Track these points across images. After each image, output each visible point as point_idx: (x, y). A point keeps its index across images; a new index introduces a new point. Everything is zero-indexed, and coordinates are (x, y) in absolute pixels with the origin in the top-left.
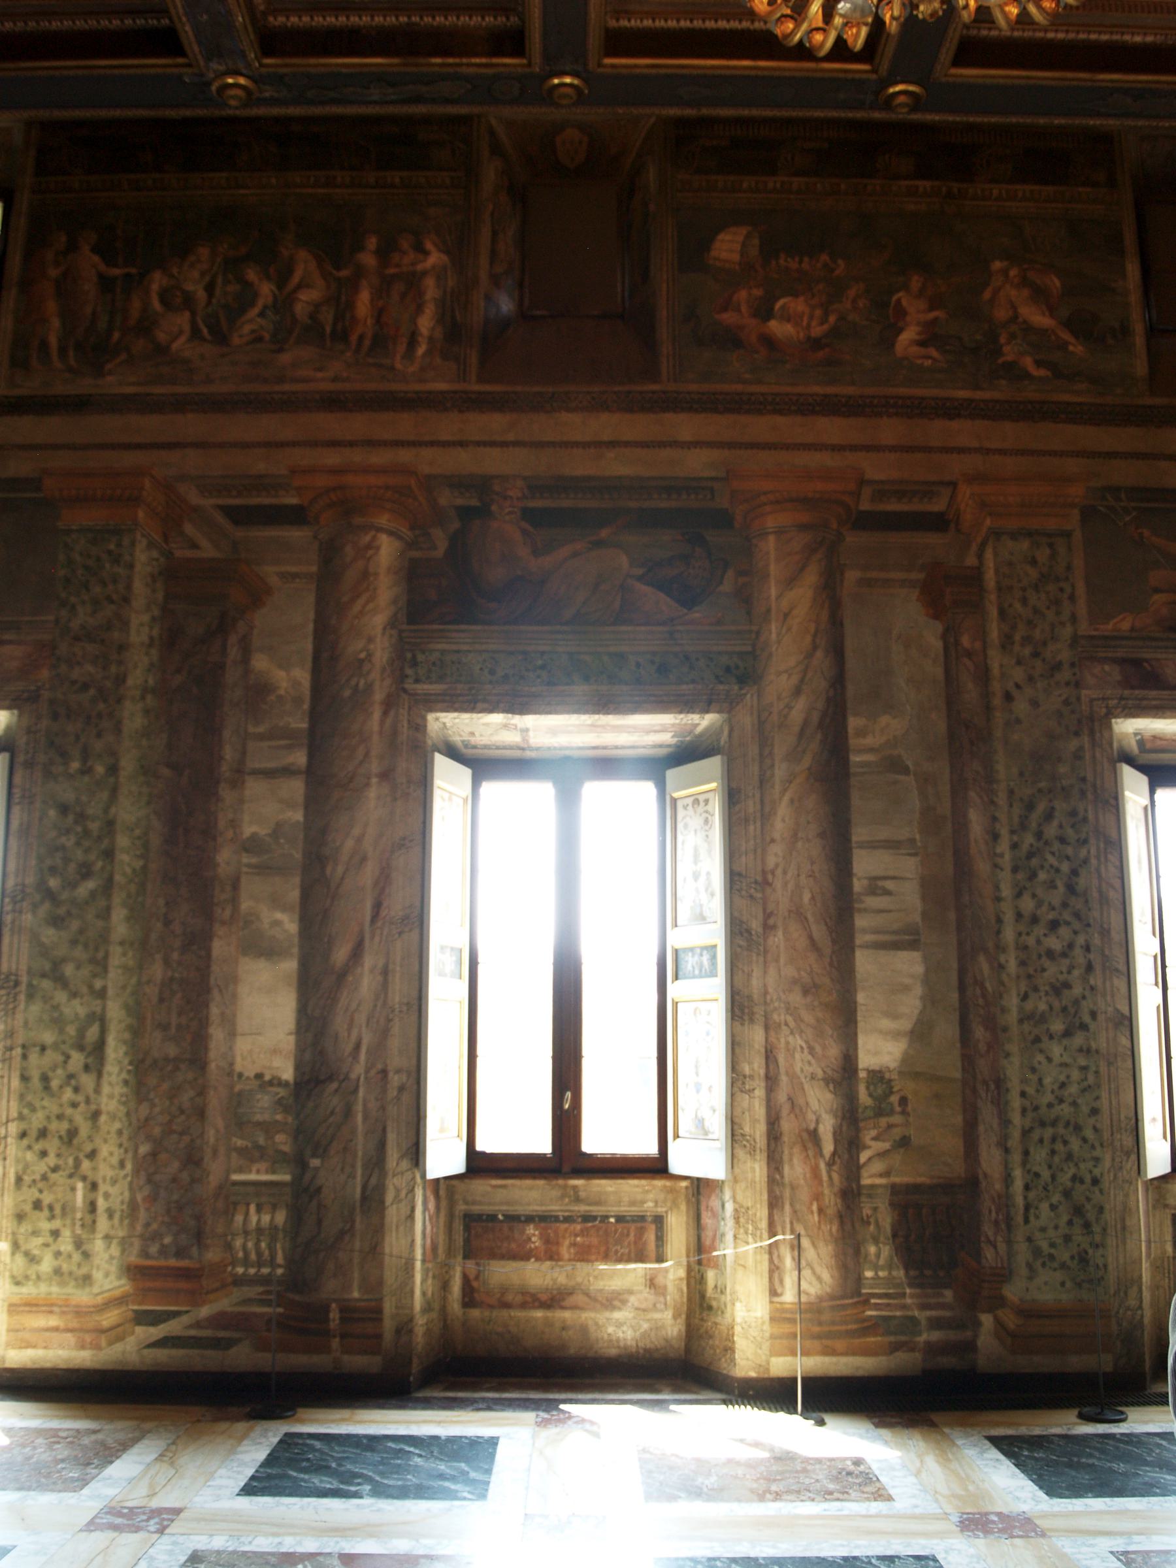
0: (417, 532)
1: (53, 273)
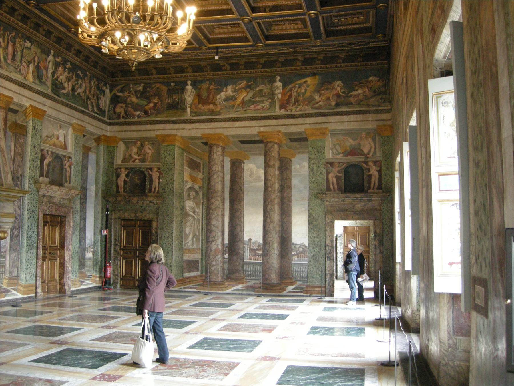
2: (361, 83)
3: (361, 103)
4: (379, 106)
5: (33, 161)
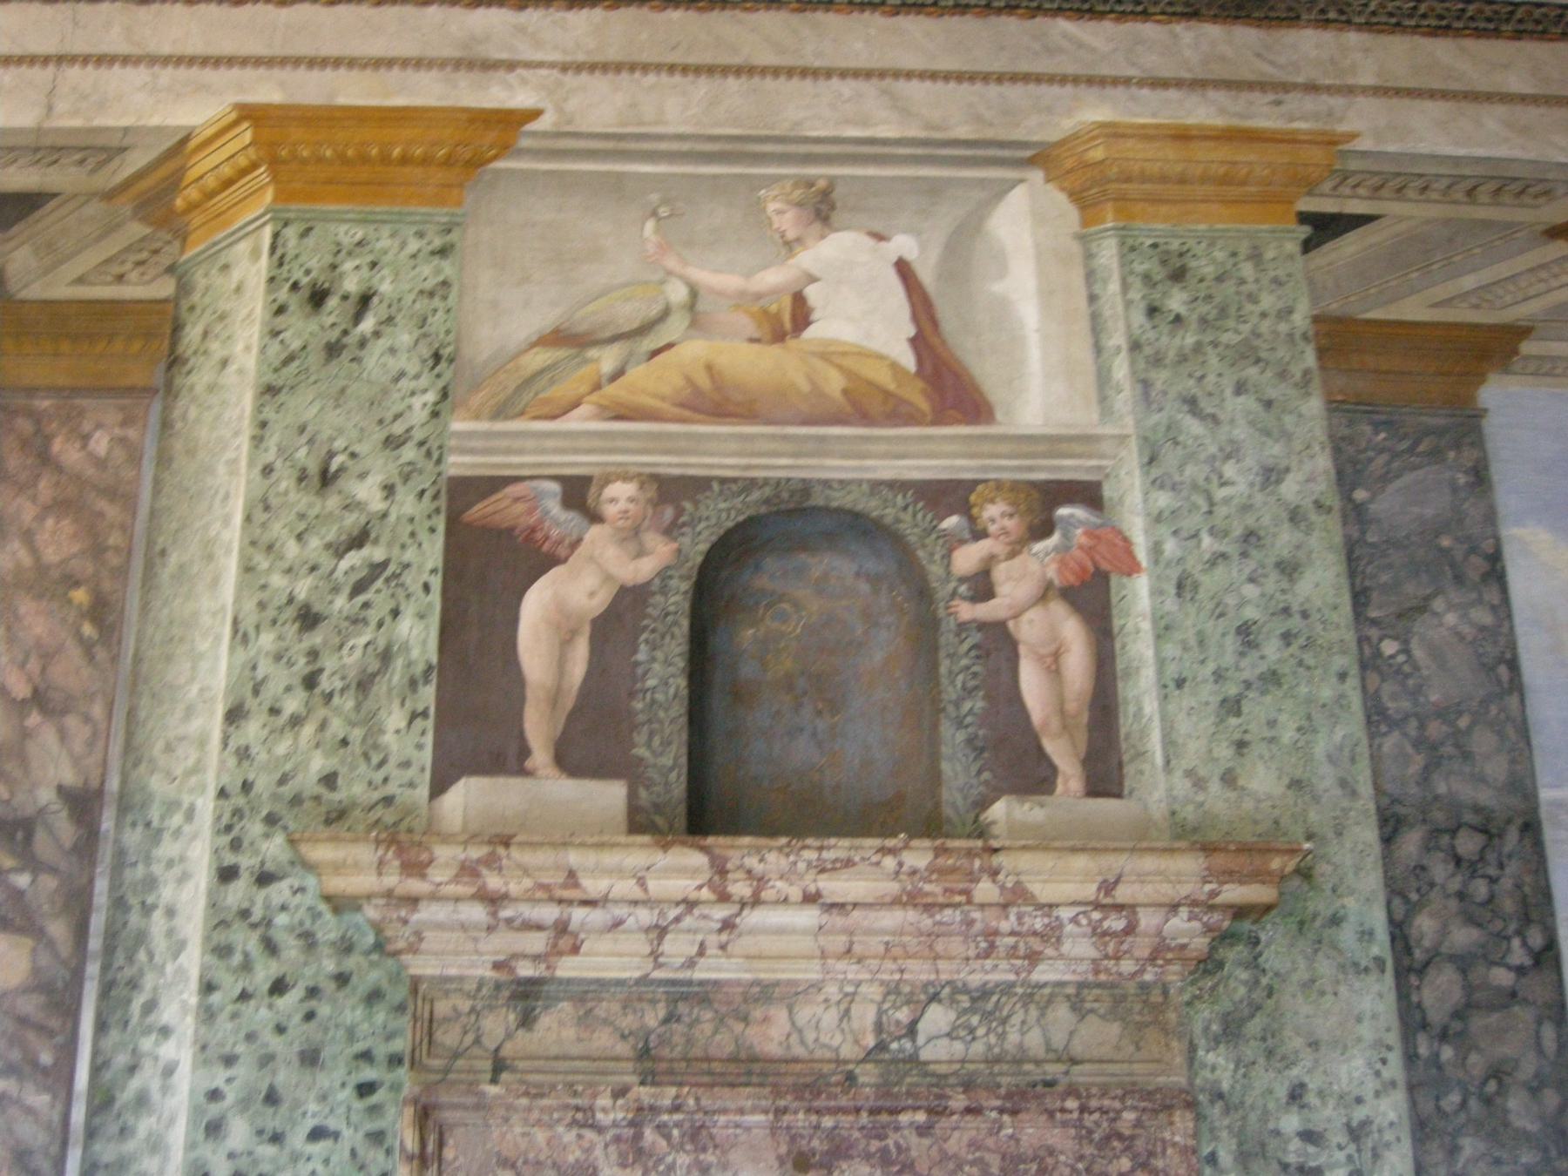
5: (309, 619)
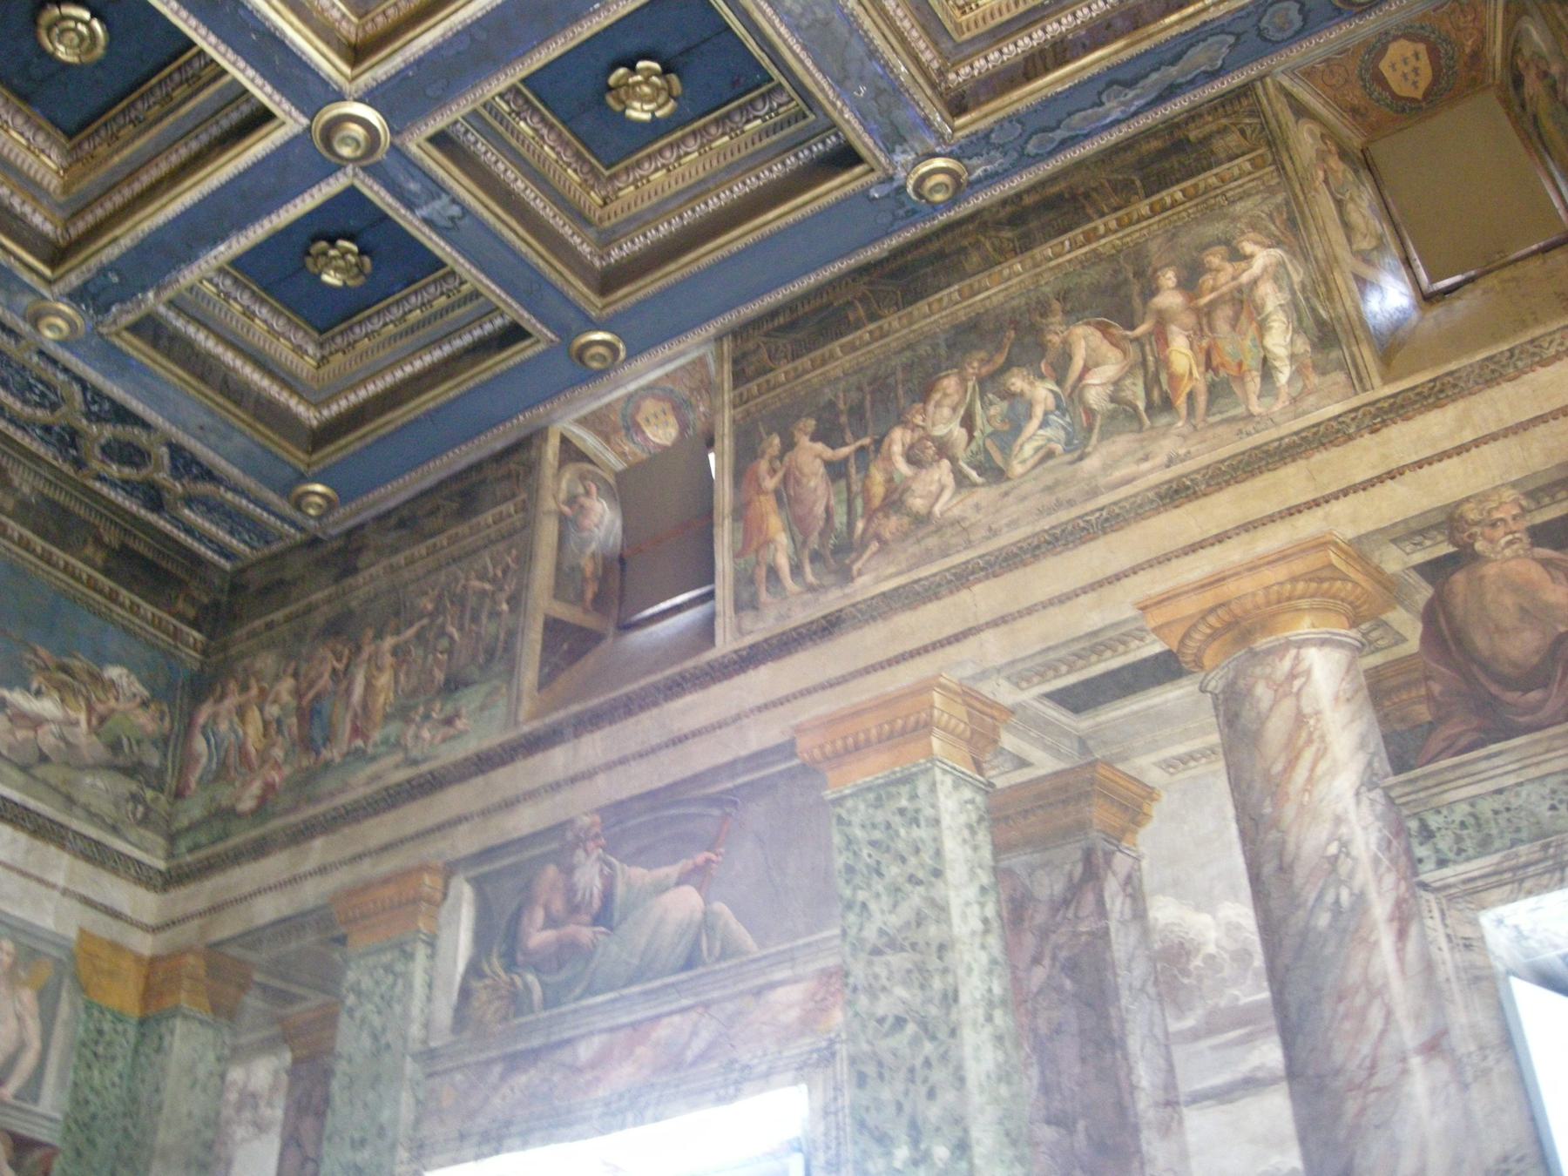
0: (1364, 627)
1: (770, 483)
2: (65, 669)
3: (41, 771)
4: (114, 830)
